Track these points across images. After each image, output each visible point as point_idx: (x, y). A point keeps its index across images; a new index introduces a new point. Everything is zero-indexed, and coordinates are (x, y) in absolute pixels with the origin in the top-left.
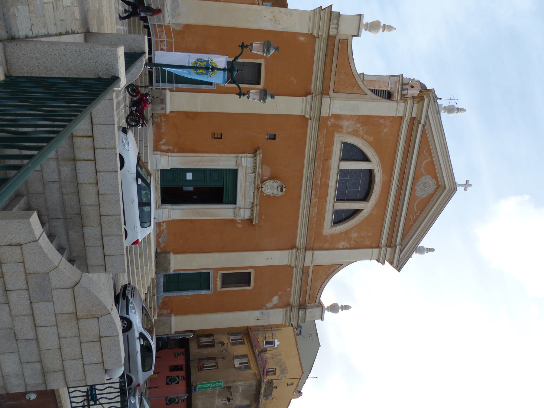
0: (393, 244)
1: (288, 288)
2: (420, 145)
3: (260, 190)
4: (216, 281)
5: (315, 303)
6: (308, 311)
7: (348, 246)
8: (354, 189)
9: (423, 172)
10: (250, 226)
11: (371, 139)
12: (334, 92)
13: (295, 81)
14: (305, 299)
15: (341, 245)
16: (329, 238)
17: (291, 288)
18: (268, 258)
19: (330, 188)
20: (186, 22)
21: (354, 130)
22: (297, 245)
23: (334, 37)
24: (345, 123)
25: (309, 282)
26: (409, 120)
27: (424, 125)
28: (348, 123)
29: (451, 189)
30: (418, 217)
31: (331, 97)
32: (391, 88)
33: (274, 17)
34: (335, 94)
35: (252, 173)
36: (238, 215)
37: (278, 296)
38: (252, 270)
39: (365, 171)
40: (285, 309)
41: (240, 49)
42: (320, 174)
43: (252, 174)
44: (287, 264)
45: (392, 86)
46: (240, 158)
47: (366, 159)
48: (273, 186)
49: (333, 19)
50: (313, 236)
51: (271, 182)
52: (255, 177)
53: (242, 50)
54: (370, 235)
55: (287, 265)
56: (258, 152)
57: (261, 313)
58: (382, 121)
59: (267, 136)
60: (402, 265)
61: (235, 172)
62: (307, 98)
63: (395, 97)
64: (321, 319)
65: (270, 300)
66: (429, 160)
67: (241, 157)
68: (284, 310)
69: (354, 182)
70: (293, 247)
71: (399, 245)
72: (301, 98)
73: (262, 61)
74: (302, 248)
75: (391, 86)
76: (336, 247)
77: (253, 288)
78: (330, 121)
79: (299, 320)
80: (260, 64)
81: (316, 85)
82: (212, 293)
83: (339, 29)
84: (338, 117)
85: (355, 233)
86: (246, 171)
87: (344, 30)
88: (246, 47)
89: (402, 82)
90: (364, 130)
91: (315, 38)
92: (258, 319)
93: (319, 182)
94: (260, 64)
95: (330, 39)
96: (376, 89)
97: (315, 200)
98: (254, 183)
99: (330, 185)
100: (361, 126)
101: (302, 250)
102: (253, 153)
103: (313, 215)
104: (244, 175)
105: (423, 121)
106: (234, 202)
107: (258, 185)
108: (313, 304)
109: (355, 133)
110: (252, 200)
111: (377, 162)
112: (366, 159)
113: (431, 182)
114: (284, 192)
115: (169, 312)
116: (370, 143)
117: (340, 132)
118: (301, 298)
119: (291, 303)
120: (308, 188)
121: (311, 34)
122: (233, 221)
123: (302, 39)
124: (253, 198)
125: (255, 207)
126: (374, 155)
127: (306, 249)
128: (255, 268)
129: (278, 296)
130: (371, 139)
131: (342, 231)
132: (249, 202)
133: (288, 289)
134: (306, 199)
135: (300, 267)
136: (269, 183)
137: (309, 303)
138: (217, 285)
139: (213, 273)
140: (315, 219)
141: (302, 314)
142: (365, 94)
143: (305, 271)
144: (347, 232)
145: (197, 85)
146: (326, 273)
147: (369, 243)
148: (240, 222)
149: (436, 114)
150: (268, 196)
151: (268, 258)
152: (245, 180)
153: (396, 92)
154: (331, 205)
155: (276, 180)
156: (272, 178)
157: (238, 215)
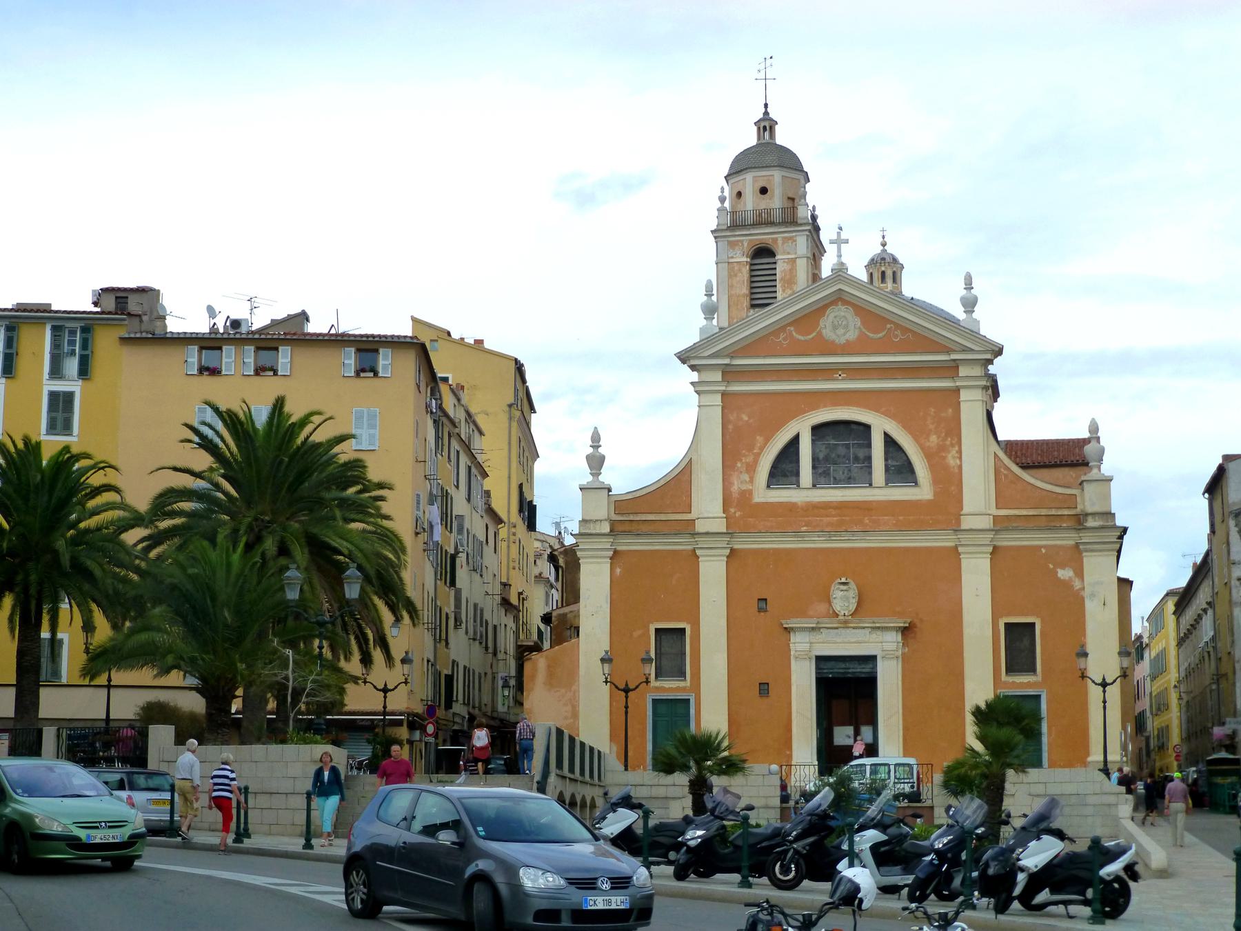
0: (953, 364)
4: (1021, 685)
6: (1090, 510)
7: (957, 448)
9: (814, 334)
11: (760, 439)
12: (691, 513)
15: (952, 461)
17: (1040, 547)
20: (608, 737)
21: (748, 471)
22: (952, 544)
23: (613, 524)
24: (736, 488)
25: (1031, 513)
26: (725, 384)
28: (736, 483)
30: (898, 326)
31: (697, 517)
40: (1084, 554)
42: (821, 520)
44: (989, 560)
47: (795, 442)
48: (841, 598)
50: (934, 517)
51: (835, 601)
54: (933, 410)
55: (991, 559)
56: (785, 626)
58: (730, 427)
61: (820, 659)
64: (1111, 480)
65: (1067, 584)
66: (792, 329)
70: (954, 553)
73: (652, 628)
76: (957, 471)
78: (735, 513)
80: (657, 630)
85: (929, 441)
87: (602, 510)
88: (606, 678)
90: (747, 453)
91: (616, 552)
92: (1104, 604)
94: (657, 630)
95: (616, 530)
100: (741, 460)
101: (959, 536)
102: (789, 632)
104: (825, 644)
105: (727, 361)
106: (873, 659)
107: (839, 622)
108: (1079, 499)
109: (751, 469)
110: (867, 631)
112: (795, 442)
113: (832, 315)
114: (849, 580)
116: (767, 440)
117: (750, 492)
119: (1072, 542)
121: (611, 558)
123: (618, 571)
124: (864, 628)
125: (878, 625)
127: (957, 531)
130: (760, 439)
131: (925, 465)
133: (1044, 551)
136: (838, 606)
137: (1076, 508)
140: (901, 518)
141: (1095, 521)
143: (1001, 525)
144: (929, 455)
147: (950, 410)
151: (977, 596)
153: (750, 240)
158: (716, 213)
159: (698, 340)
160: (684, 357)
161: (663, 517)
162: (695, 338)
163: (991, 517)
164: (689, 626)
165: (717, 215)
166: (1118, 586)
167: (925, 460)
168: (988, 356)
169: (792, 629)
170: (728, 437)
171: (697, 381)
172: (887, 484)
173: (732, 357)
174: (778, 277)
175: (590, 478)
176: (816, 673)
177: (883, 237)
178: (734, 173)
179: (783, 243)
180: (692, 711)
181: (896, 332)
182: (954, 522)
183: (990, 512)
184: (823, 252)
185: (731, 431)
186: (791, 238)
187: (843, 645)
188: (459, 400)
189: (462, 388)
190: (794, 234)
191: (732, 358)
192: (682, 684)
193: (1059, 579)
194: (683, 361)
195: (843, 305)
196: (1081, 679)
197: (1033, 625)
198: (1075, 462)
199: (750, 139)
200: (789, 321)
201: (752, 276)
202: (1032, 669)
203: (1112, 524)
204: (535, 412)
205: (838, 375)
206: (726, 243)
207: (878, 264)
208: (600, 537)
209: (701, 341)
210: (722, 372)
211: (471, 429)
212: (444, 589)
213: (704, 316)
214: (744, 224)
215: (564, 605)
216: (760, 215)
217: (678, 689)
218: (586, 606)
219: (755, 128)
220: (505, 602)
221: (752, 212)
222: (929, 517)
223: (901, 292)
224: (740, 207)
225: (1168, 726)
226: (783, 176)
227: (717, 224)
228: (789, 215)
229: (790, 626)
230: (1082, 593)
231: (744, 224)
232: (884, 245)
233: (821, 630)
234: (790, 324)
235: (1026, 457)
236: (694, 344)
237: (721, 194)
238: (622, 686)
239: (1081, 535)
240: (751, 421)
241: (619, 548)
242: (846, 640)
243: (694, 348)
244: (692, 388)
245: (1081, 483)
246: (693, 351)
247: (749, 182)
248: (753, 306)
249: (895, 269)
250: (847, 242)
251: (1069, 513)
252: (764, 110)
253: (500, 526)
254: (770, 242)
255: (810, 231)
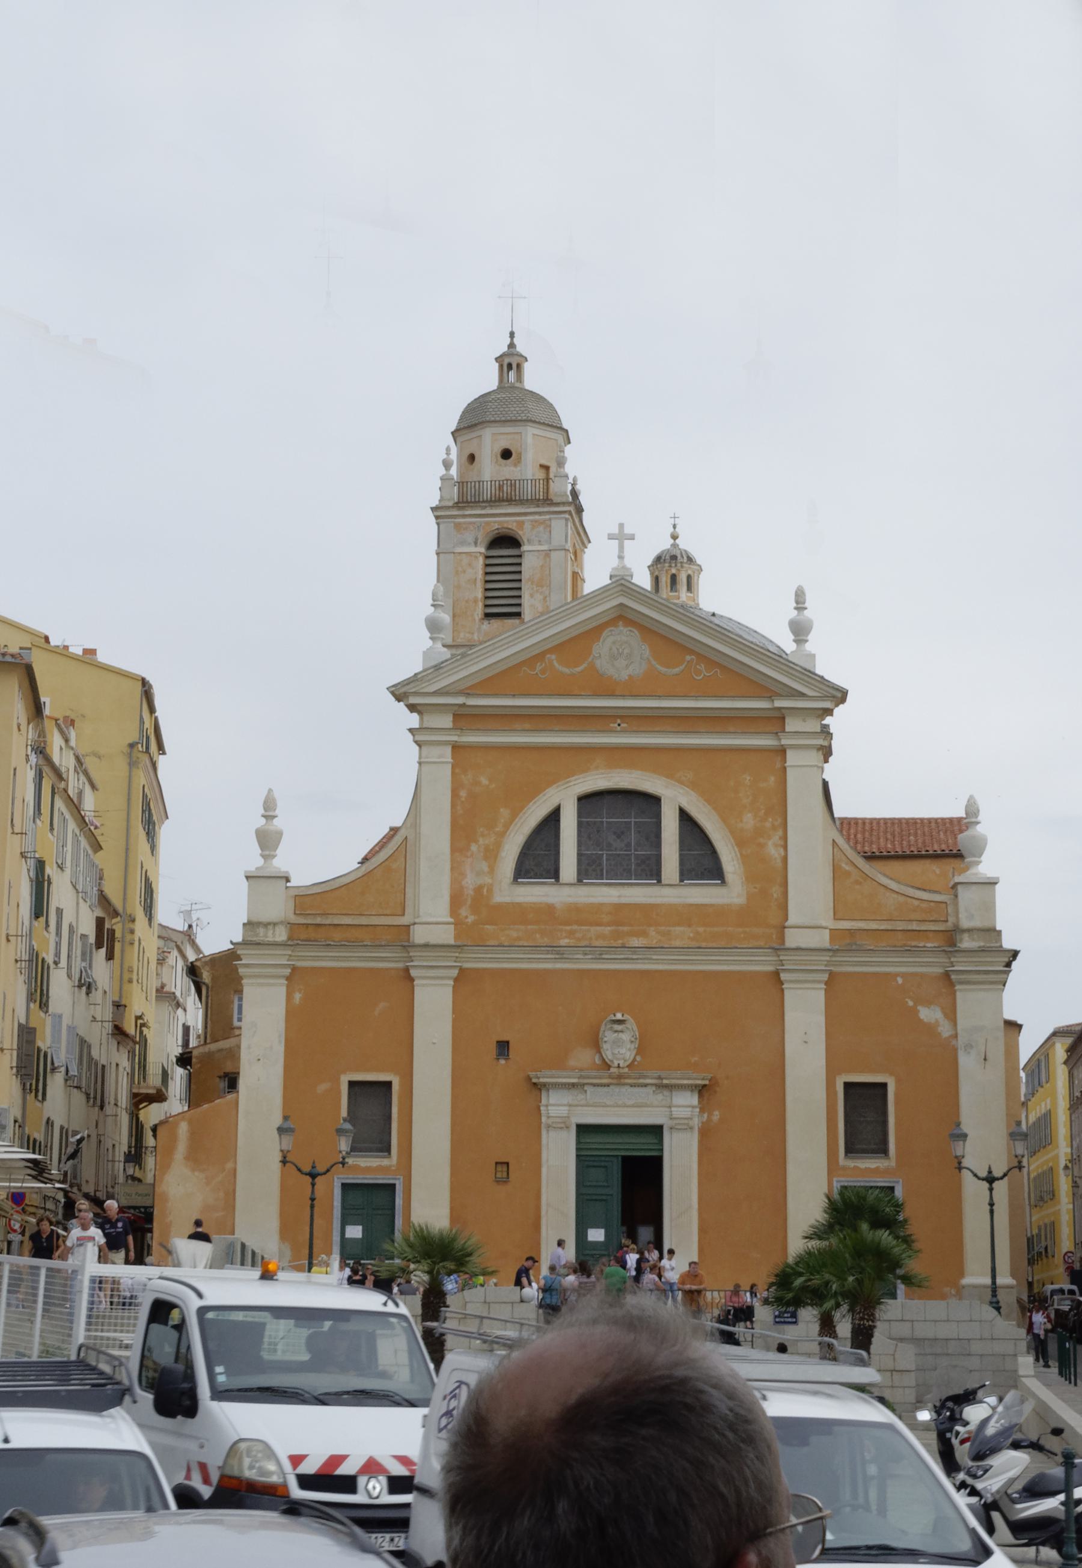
0: (777, 714)
1: (897, 982)
2: (514, 695)
3: (626, 1070)
5: (946, 903)
6: (965, 923)
7: (780, 833)
8: (631, 832)
10: (718, 1089)
11: (505, 813)
12: (403, 915)
13: (382, 1005)
14: (931, 935)
15: (773, 851)
16: (755, 888)
17: (897, 975)
18: (806, 1042)
19: (623, 900)
21: (486, 858)
22: (771, 968)
23: (292, 927)
24: (470, 882)
25: (882, 928)
27: (466, 693)
29: (622, 591)
30: (701, 657)
31: (412, 922)
32: (476, 544)
33: (259, 1060)
34: (406, 913)
35: (586, 1091)
36: (686, 1121)
37: (919, 1008)
38: (837, 1078)
39: (580, 815)
40: (957, 988)
41: (288, 1165)
43: (588, 1092)
44: (823, 992)
45: (470, 538)
46: (550, 1121)
47: (553, 818)
48: (614, 1042)
49: (257, 935)
50: (747, 930)
51: (605, 1046)
52: (594, 1085)
53: (289, 1162)
54: (748, 778)
55: (826, 990)
56: (534, 1080)
57: (966, 1050)
58: (463, 794)
59: (500, 1060)
60: (828, 686)
61: (583, 1130)
62: (417, 977)
63: (505, 526)
64: (996, 883)
65: (930, 1029)
66: (553, 657)
67: (548, 1117)
68: (961, 990)
69: (615, 837)
71: (773, 701)
72: (418, 991)
73: (345, 1080)
74: (779, 956)
75: (469, 544)
77: (891, 1074)
78: (466, 917)
79: (992, 945)
80: (352, 1084)
81: (388, 961)
82: (901, 1180)
83: (275, 921)
84: (456, 900)
85: (741, 821)
86: (582, 1106)
87: (278, 908)
89: (453, 507)
92: (985, 1059)
93: (607, 930)
94: (352, 1084)
96: (480, 594)
97: (653, 937)
98: (608, 1086)
99: (615, 900)
100: (476, 842)
101: (781, 958)
102: (540, 1090)
103: (691, 935)
104: (590, 1108)
105: (460, 700)
106: (656, 1131)
108: (950, 910)
109: (492, 855)
110: (650, 1090)
111: (560, 789)
112: (553, 818)
113: (610, 640)
114: (626, 1017)
115: (953, 1292)
116: (514, 815)
117: (490, 890)
118: (929, 945)
119: (941, 970)
120: (622, 956)
121: (288, 978)
122: (705, 1133)
123: (297, 997)
124: (646, 1085)
125: (665, 1082)
126: (545, 798)
127: (779, 947)
128: (831, 1073)
129: (919, 1008)
130: (505, 813)
131: (736, 855)
132: (657, 1094)
133: (900, 980)
134: (648, 959)
135: (830, 956)
138: (878, 1168)
139: (843, 1179)
140: (701, 929)
141: (973, 940)
142: (404, 843)
144: (740, 842)
145: (396, 1217)
146: (857, 882)
147: (772, 779)
148: (708, 1116)
149: (441, 671)
150: (640, 1051)
151: (806, 1042)
152: (603, 1106)
153: (488, 523)
154: (666, 891)
155: (600, 1036)
156: (596, 1044)
157: (686, 1121)
158: (439, 484)
159: (421, 669)
160: (399, 693)
161: (363, 921)
162: (415, 666)
163: (828, 931)
164: (398, 1078)
165: (440, 485)
166: (1006, 1035)
167: (736, 849)
168: (827, 705)
169: (544, 1085)
170: (459, 808)
171: (417, 726)
172: (681, 880)
173: (468, 694)
174: (525, 576)
175: (260, 862)
176: (578, 1149)
177: (674, 526)
178: (465, 428)
179: (533, 527)
180: (399, 1201)
181: (698, 667)
182: (774, 936)
183: (824, 924)
184: (586, 541)
185: (463, 799)
186: (543, 522)
187: (616, 1109)
188: (67, 741)
189: (72, 723)
190: (548, 517)
191: (468, 695)
192: (385, 1162)
193: (921, 1021)
194: (399, 699)
195: (625, 626)
196: (957, 1170)
197: (884, 1086)
198: (939, 852)
199: (488, 380)
200: (550, 646)
201: (487, 573)
202: (882, 1150)
203: (998, 945)
204: (164, 753)
205: (616, 725)
206: (453, 524)
207: (667, 565)
208: (270, 947)
209: (424, 671)
210: (454, 715)
211: (81, 782)
212: (37, 1014)
213: (429, 635)
214: (477, 500)
215: (208, 1041)
216: (501, 487)
217: (380, 1169)
218: (249, 1047)
219: (497, 365)
220: (119, 1032)
221: (489, 483)
222: (741, 930)
223: (698, 604)
224: (472, 476)
225: (1053, 1223)
226: (534, 435)
227: (439, 498)
228: (541, 490)
229: (542, 1080)
230: (954, 1042)
231: (477, 500)
232: (675, 537)
233: (586, 1088)
234: (550, 651)
235: (871, 843)
236: (416, 675)
237: (445, 456)
238: (307, 1169)
239: (952, 960)
240: (493, 786)
241: (299, 964)
242: (620, 1103)
243: (415, 679)
244: (411, 737)
245: (955, 886)
246: (412, 685)
247: (489, 442)
248: (488, 616)
249: (690, 572)
250: (632, 537)
251: (937, 929)
252: (508, 341)
253: (114, 921)
254: (514, 526)
255: (570, 513)
